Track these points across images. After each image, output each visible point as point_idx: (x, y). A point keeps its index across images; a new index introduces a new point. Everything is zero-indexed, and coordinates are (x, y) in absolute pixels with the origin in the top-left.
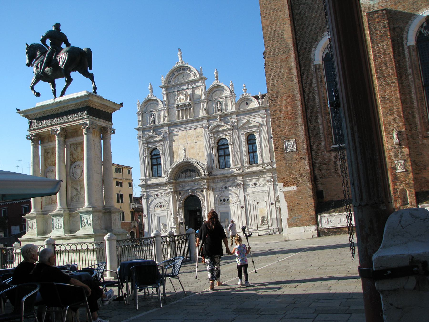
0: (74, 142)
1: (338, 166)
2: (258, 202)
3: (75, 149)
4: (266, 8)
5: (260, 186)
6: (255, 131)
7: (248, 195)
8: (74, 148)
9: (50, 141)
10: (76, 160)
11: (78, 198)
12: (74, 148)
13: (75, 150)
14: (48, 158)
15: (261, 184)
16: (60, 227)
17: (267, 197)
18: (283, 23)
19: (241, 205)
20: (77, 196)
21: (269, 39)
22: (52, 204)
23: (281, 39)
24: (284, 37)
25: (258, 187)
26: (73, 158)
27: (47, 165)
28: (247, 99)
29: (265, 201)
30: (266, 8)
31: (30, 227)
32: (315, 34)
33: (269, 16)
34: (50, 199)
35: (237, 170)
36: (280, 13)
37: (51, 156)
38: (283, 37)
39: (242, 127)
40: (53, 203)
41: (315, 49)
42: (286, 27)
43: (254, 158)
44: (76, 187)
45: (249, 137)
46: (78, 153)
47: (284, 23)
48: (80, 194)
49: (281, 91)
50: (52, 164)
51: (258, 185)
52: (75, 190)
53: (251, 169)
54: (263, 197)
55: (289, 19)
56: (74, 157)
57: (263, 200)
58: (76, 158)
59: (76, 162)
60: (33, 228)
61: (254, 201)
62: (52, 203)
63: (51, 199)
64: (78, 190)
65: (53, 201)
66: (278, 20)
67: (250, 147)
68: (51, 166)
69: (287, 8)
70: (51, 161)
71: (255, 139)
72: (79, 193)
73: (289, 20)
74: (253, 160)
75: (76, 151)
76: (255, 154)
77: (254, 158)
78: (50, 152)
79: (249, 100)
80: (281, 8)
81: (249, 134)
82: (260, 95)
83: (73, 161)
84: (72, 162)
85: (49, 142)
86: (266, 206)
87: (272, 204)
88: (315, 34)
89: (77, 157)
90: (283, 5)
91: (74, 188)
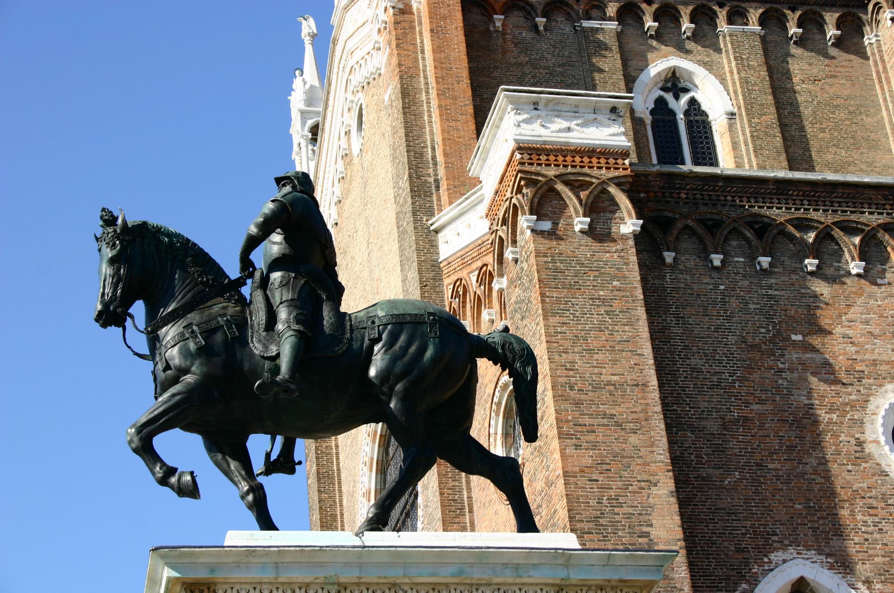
4: (578, 403)
18: (645, 477)
21: (592, 525)
23: (640, 540)
24: (654, 533)
30: (578, 403)
32: (739, 550)
33: (591, 437)
36: (633, 439)
38: (648, 533)
42: (659, 496)
47: (651, 478)
55: (668, 471)
66: (625, 461)
69: (658, 426)
73: (671, 474)
80: (636, 421)
88: (739, 550)
90: (644, 411)
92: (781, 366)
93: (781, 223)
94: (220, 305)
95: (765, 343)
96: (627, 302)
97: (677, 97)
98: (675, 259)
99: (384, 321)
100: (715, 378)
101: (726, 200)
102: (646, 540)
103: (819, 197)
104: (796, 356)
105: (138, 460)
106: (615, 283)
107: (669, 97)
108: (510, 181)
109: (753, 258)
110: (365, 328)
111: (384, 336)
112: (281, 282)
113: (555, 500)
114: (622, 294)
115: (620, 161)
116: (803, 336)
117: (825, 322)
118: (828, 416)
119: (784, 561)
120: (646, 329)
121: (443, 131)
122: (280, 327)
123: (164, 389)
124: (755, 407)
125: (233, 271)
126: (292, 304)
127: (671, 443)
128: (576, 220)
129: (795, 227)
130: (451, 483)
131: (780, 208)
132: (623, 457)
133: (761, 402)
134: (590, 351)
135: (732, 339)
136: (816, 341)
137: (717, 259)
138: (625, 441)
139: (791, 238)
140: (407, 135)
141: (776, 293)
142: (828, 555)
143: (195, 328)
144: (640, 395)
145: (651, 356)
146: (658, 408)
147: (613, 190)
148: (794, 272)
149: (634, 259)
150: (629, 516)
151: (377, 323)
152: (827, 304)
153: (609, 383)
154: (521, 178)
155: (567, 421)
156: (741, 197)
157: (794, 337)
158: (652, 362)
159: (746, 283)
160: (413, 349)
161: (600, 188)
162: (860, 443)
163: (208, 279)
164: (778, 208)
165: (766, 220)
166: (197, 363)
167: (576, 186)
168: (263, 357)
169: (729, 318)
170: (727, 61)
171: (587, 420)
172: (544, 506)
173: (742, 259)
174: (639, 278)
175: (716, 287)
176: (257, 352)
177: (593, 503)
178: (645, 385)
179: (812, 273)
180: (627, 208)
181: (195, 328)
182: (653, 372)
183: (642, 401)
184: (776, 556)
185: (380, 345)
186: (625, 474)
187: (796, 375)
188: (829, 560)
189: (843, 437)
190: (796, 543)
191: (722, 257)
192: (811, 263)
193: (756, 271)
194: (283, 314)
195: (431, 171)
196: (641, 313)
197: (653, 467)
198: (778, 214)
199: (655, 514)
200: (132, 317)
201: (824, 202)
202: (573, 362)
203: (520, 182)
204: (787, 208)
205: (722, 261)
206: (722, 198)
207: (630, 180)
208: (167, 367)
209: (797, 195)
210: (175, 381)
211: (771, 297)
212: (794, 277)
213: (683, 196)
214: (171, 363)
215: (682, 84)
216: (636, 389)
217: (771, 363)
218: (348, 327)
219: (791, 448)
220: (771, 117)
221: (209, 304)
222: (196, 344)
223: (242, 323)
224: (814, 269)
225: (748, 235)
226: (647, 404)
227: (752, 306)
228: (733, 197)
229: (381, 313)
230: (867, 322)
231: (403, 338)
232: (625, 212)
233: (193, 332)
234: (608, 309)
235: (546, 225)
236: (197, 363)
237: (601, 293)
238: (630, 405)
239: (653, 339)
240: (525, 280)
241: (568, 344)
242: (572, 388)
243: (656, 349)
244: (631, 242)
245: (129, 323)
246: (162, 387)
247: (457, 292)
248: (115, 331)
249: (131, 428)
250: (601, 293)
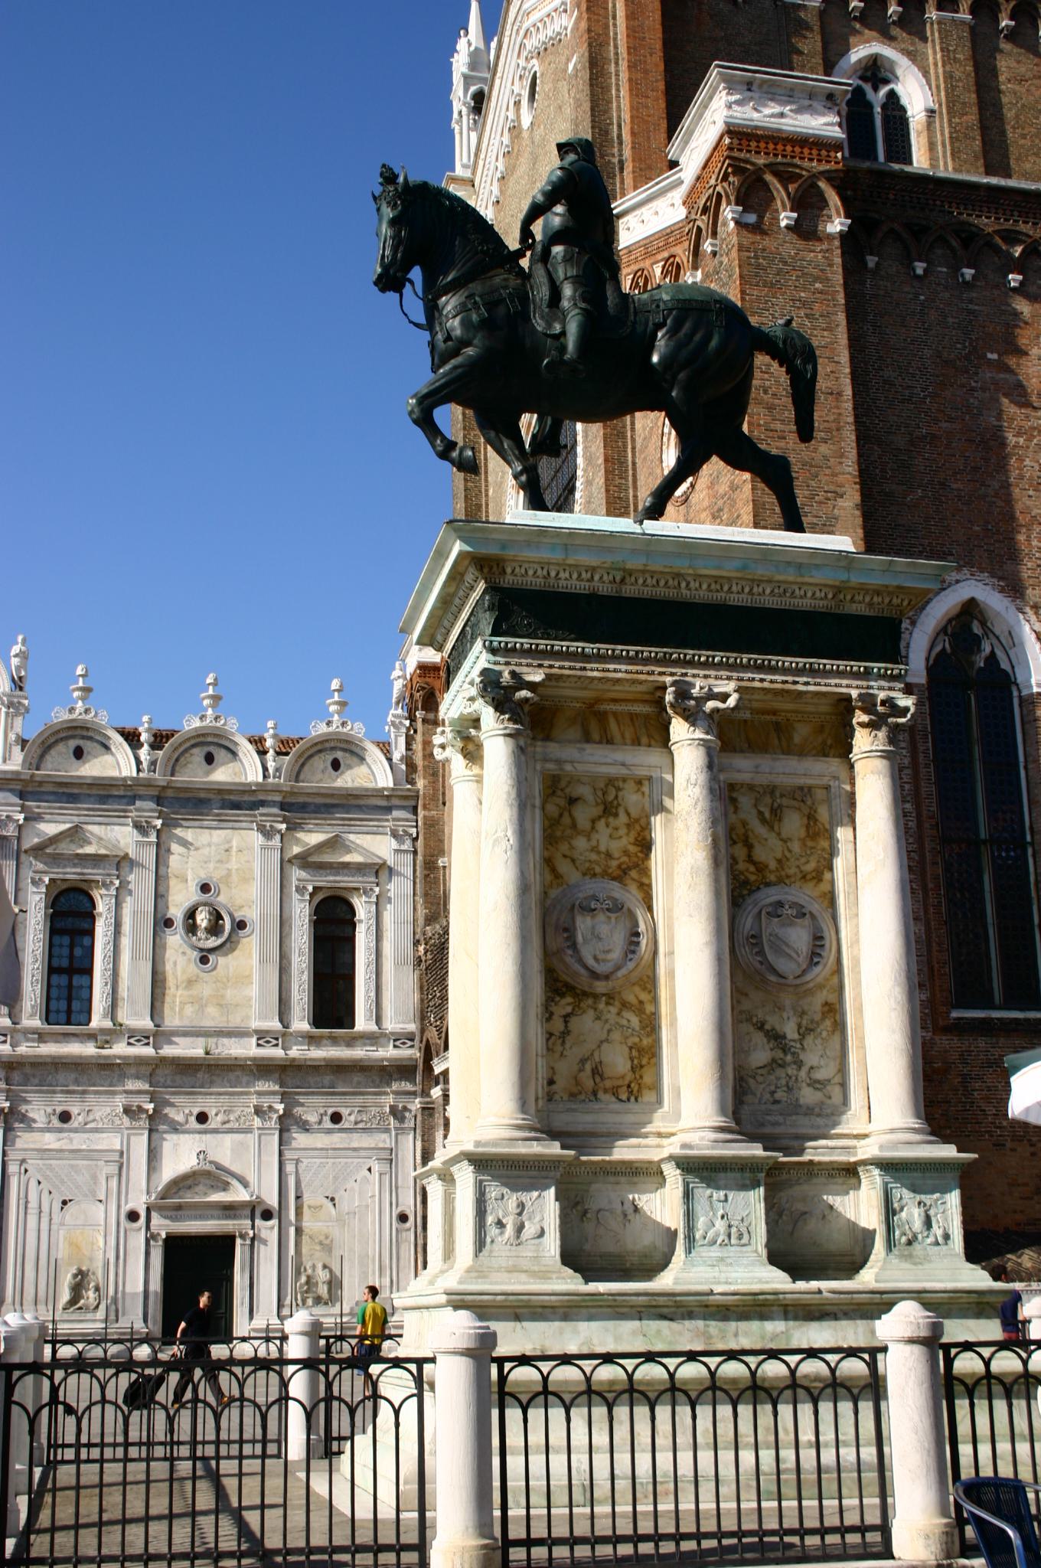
0: (762, 780)
1: (975, 1093)
2: (64, 1203)
3: (767, 815)
5: (81, 1130)
6: (99, 878)
7: (23, 1161)
8: (761, 813)
9: (596, 736)
10: (772, 878)
11: (783, 1082)
12: (761, 813)
13: (763, 820)
14: (574, 826)
15: (91, 1117)
16: (740, 1236)
17: (114, 1183)
18: (832, 488)
19: (400, 1209)
20: (781, 1073)
22: (601, 1095)
25: (76, 1131)
26: (750, 859)
27: (564, 867)
28: (85, 733)
29: (103, 1198)
31: (500, 1224)
34: (588, 1067)
35: (259, 1045)
37: (593, 821)
39: (38, 850)
40: (606, 1091)
41: (913, 623)
42: (844, 509)
43: (69, 1000)
44: (772, 1021)
45: (62, 899)
46: (785, 841)
47: (840, 490)
48: (799, 1064)
50: (598, 870)
51: (74, 1123)
52: (761, 1034)
53: (318, 1053)
54: (95, 1178)
55: (855, 483)
56: (756, 858)
57: (93, 1193)
58: (773, 865)
59: (768, 885)
60: (530, 1230)
61: (45, 1194)
62: (595, 1093)
63: (588, 1067)
64: (784, 1037)
65: (608, 1084)
66: (813, 470)
67: (61, 946)
68: (594, 875)
70: (595, 849)
71: (92, 918)
72: (789, 1058)
73: (858, 486)
74: (63, 1005)
75: (772, 828)
76: (77, 980)
77: (69, 1000)
78: (590, 798)
79: (90, 738)
80: (828, 430)
81: (64, 886)
82: (275, 736)
83: (752, 878)
84: (746, 882)
85: (587, 738)
86: (102, 1223)
87: (133, 1216)
89: (779, 861)
90: (837, 421)
91: (761, 1026)
92: (973, 384)
93: (989, 234)
94: (502, 277)
95: (960, 359)
96: (828, 306)
97: (876, 89)
98: (878, 264)
99: (670, 305)
100: (907, 392)
101: (935, 205)
103: (1030, 208)
104: (989, 375)
105: (418, 431)
106: (817, 285)
107: (868, 88)
108: (716, 167)
109: (956, 269)
110: (649, 312)
111: (668, 322)
112: (564, 256)
113: (740, 504)
114: (823, 297)
115: (832, 154)
116: (999, 355)
117: (1023, 342)
118: (1015, 439)
119: (958, 582)
120: (845, 336)
121: (632, 108)
122: (565, 304)
123: (443, 362)
124: (944, 425)
125: (513, 243)
126: (576, 281)
127: (859, 455)
128: (783, 215)
129: (1003, 238)
130: (618, 481)
131: (988, 218)
132: (811, 466)
133: (950, 420)
135: (927, 352)
136: (1012, 362)
137: (920, 268)
139: (997, 250)
140: (592, 109)
141: (976, 308)
142: (1000, 579)
143: (477, 299)
144: (833, 404)
145: (848, 364)
146: (851, 419)
147: (822, 185)
148: (997, 287)
149: (838, 260)
151: (662, 306)
152: (1026, 323)
154: (729, 165)
155: (759, 425)
156: (950, 203)
157: (990, 356)
158: (848, 370)
159: (947, 295)
160: (698, 337)
161: (809, 182)
163: (488, 249)
164: (987, 217)
165: (974, 229)
166: (479, 336)
167: (785, 178)
168: (545, 334)
170: (933, 53)
171: (779, 426)
172: (726, 510)
173: (945, 270)
174: (842, 282)
175: (916, 295)
176: (539, 329)
178: (840, 394)
179: (1014, 289)
180: (836, 205)
181: (477, 299)
182: (848, 381)
183: (835, 411)
185: (664, 330)
186: (813, 483)
187: (987, 394)
188: (1001, 583)
189: (1027, 462)
191: (925, 265)
192: (1014, 279)
193: (958, 283)
194: (567, 291)
195: (616, 150)
196: (841, 318)
197: (841, 479)
198: (987, 223)
199: (839, 526)
200: (412, 282)
201: (1035, 214)
203: (727, 169)
204: (996, 218)
205: (925, 270)
206: (931, 202)
207: (842, 175)
208: (448, 338)
209: (1008, 205)
210: (456, 353)
211: (972, 312)
212: (996, 292)
213: (891, 197)
214: (453, 334)
215: (883, 74)
216: (830, 398)
217: (964, 381)
218: (632, 310)
219: (976, 469)
220: (972, 118)
221: (490, 274)
222: (479, 315)
223: (523, 298)
224: (1017, 285)
225: (954, 244)
226: (840, 414)
227: (950, 320)
228: (942, 202)
229: (665, 297)
231: (687, 327)
232: (833, 212)
233: (475, 303)
234: (808, 312)
235: (751, 218)
236: (479, 336)
237: (803, 294)
238: (824, 414)
239: (850, 347)
240: (723, 275)
242: (766, 392)
243: (852, 359)
244: (837, 243)
245: (407, 289)
246: (439, 358)
247: (637, 283)
248: (393, 296)
249: (412, 398)
250: (803, 294)
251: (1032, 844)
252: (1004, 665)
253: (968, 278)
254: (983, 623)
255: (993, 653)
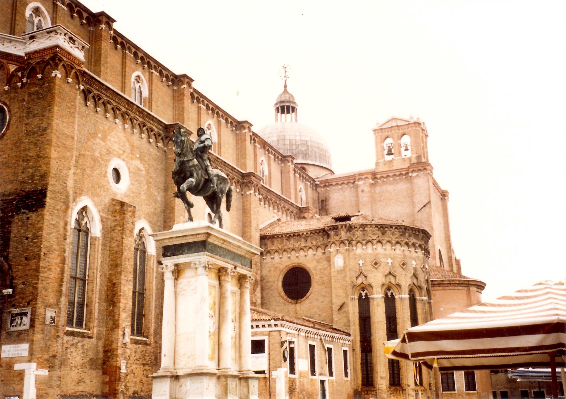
33: (58, 149)
49: (55, 247)
102: (65, 185)
133: (88, 151)
134: (63, 122)
135: (86, 129)
137: (89, 103)
138: (66, 153)
142: (93, 201)
150: (63, 176)
153: (66, 134)
162: (106, 172)
169: (87, 122)
171: (58, 143)
175: (85, 112)
177: (56, 169)
184: (83, 197)
190: (88, 195)
202: (59, 124)
211: (97, 121)
230: (114, 137)
241: (58, 117)
242: (57, 132)
251: (88, 280)
252: (88, 226)
253: (98, 111)
254: (86, 213)
255: (86, 222)
